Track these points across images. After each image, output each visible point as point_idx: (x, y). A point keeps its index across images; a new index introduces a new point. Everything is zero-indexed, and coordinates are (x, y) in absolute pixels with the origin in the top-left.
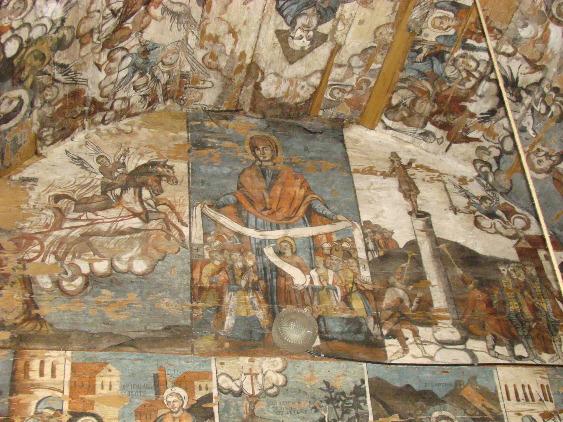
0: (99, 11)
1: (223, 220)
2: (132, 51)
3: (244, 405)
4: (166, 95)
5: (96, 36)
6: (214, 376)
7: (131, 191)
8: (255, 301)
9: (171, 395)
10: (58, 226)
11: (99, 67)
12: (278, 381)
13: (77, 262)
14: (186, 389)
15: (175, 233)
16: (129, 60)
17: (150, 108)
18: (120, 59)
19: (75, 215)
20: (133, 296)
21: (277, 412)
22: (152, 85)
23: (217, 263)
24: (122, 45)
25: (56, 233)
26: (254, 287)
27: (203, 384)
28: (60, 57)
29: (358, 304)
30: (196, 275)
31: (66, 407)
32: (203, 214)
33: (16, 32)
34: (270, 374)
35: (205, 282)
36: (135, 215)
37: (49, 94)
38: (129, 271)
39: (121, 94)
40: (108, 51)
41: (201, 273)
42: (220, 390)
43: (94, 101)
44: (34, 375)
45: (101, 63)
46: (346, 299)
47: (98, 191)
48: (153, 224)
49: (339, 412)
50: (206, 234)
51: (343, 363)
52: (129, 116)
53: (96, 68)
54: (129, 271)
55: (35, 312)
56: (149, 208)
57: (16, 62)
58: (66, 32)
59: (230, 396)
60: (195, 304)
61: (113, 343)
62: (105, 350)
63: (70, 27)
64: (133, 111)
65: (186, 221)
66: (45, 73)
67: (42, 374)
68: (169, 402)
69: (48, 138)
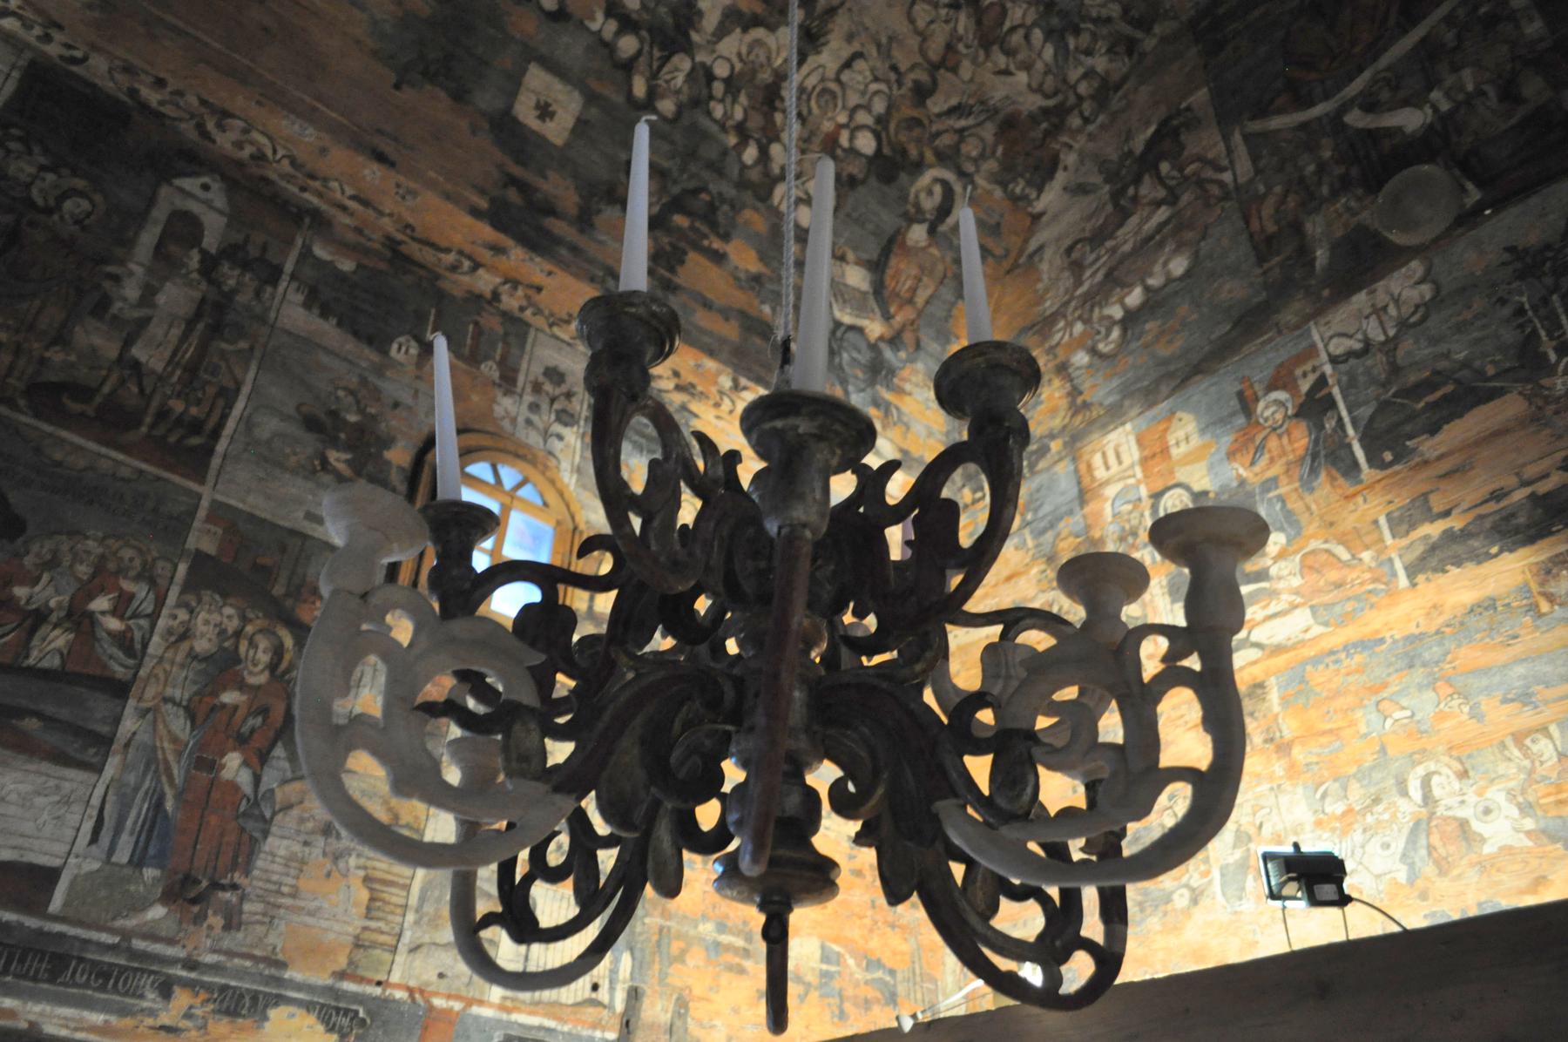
0: (932, 22)
1: (1276, 123)
2: (1029, 21)
3: (1377, 362)
4: (1144, 24)
5: (961, 47)
6: (1320, 345)
7: (1147, 179)
8: (1353, 204)
9: (1267, 407)
10: (1078, 283)
11: (1006, 72)
12: (1422, 297)
13: (1108, 311)
14: (1284, 388)
15: (1215, 190)
16: (1037, 34)
17: (1136, 56)
18: (1023, 41)
19: (1093, 256)
20: (1184, 309)
21: (1434, 341)
22: (1105, 31)
23: (1278, 189)
24: (1007, 25)
25: (1079, 292)
26: (1345, 184)
27: (1308, 367)
28: (936, 105)
29: (1533, 88)
30: (1255, 225)
31: (1144, 492)
32: (1247, 138)
33: (852, 125)
34: (1406, 294)
35: (1271, 228)
36: (1158, 204)
37: (971, 148)
38: (1170, 280)
39: (1074, 74)
40: (995, 48)
41: (1260, 218)
42: (1334, 360)
43: (1045, 112)
44: (1100, 473)
45: (1003, 66)
46: (1510, 94)
47: (1109, 208)
48: (1186, 198)
49: (1549, 281)
50: (1255, 159)
51: (1534, 201)
52: (1117, 87)
53: (1003, 78)
54: (1170, 280)
55: (1079, 400)
56: (1173, 183)
57: (886, 151)
58: (912, 76)
59: (1352, 361)
60: (1266, 266)
61: (1173, 384)
62: (1167, 398)
63: (913, 67)
64: (1116, 77)
65: (1225, 162)
66: (938, 134)
67: (1108, 468)
68: (1266, 420)
69: (1027, 191)
